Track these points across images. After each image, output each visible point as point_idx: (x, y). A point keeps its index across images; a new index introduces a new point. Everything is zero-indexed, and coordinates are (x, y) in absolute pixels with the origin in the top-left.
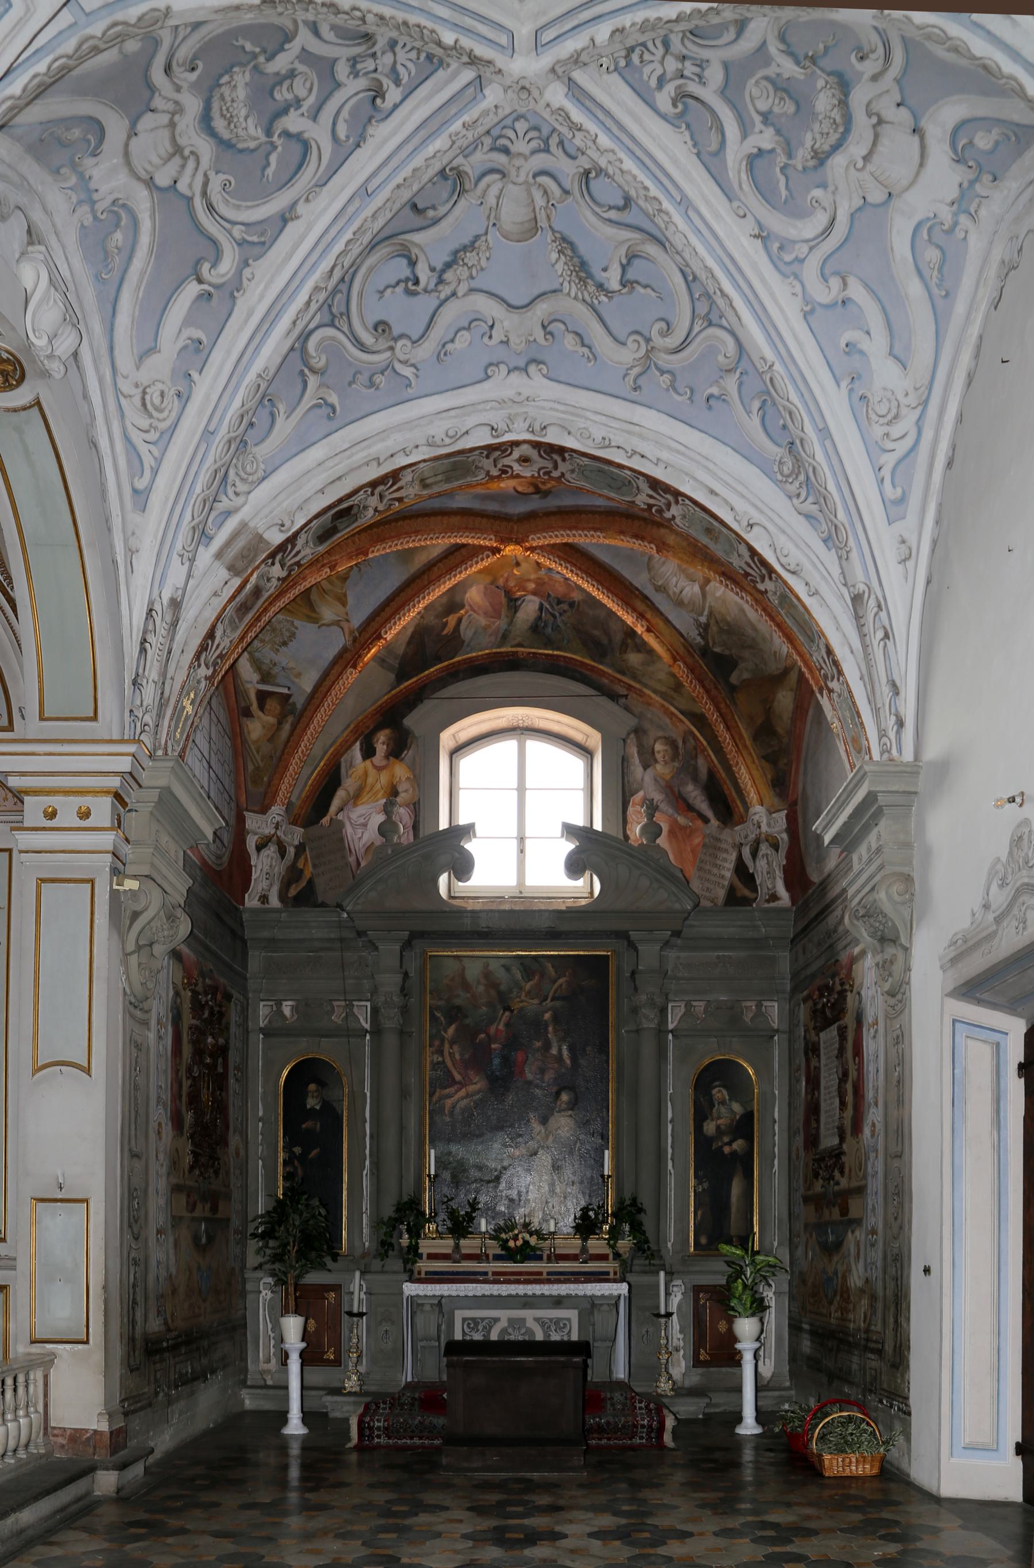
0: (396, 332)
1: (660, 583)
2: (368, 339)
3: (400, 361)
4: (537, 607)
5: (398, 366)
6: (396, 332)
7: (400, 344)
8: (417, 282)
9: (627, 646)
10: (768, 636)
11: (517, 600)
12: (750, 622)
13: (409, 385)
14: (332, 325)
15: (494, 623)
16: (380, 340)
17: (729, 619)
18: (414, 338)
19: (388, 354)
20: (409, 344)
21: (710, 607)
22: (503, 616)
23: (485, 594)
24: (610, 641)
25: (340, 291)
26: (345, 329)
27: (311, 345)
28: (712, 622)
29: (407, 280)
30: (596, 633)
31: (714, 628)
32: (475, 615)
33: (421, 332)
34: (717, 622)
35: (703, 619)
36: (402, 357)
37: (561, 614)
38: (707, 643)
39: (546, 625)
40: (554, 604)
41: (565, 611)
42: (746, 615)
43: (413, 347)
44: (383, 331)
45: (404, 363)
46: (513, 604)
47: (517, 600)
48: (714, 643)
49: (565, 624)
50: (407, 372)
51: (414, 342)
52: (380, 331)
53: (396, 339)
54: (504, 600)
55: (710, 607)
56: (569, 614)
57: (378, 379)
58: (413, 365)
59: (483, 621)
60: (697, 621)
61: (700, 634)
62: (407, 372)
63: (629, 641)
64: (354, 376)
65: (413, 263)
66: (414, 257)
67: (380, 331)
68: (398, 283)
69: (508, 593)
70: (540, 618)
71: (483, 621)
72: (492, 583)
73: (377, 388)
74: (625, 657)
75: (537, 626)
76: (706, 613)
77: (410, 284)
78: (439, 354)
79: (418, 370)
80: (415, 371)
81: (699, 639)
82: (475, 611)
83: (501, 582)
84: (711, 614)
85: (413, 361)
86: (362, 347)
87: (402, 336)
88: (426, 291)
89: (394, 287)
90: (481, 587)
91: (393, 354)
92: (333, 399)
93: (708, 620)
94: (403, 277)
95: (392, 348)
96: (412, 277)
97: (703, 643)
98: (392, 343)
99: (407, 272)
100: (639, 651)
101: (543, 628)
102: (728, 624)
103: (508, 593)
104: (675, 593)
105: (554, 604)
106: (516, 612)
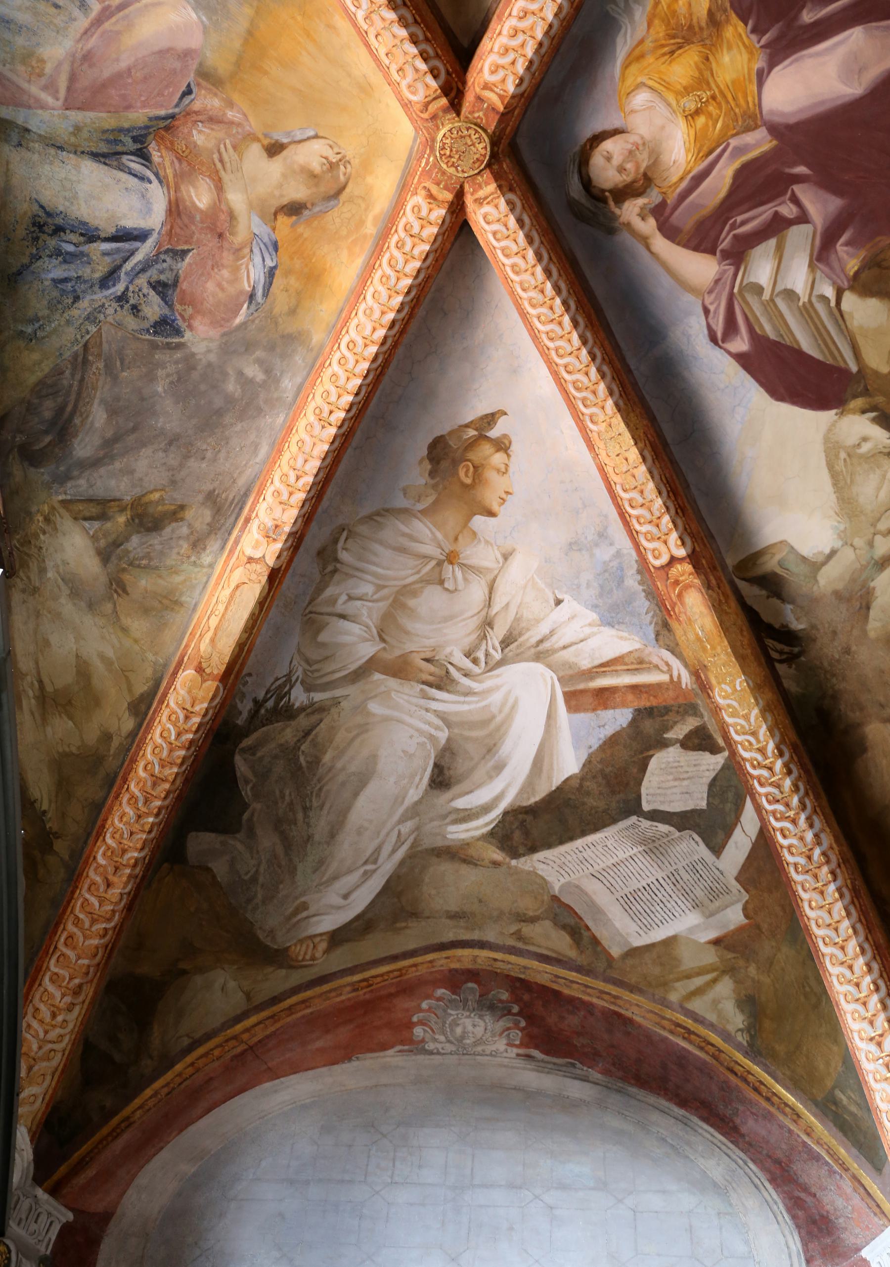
1: (344, 556)
4: (131, 222)
9: (103, 517)
10: (333, 867)
11: (143, 155)
12: (344, 813)
15: (50, 87)
17: (327, 758)
21: (336, 702)
22: (76, 116)
23: (163, 53)
24: (95, 463)
28: (303, 721)
30: (98, 416)
31: (288, 733)
32: (83, 22)
34: (307, 733)
35: (299, 696)
37: (122, 299)
38: (246, 732)
39: (69, 259)
40: (153, 274)
41: (135, 309)
42: (356, 794)
46: (128, 148)
47: (143, 155)
48: (252, 750)
49: (91, 318)
54: (138, 116)
55: (336, 702)
56: (131, 323)
59: (57, 51)
60: (289, 680)
61: (258, 704)
63: (122, 519)
69: (166, 126)
70: (91, 236)
71: (57, 51)
72: (206, 75)
74: (66, 523)
75: (59, 230)
76: (318, 697)
81: (246, 707)
82: (98, 22)
83: (206, 101)
84: (321, 709)
90: (195, 41)
93: (303, 709)
97: (240, 722)
100: (105, 556)
101: (58, 253)
102: (316, 762)
103: (166, 126)
104: (333, 601)
105: (153, 274)
106: (96, 156)
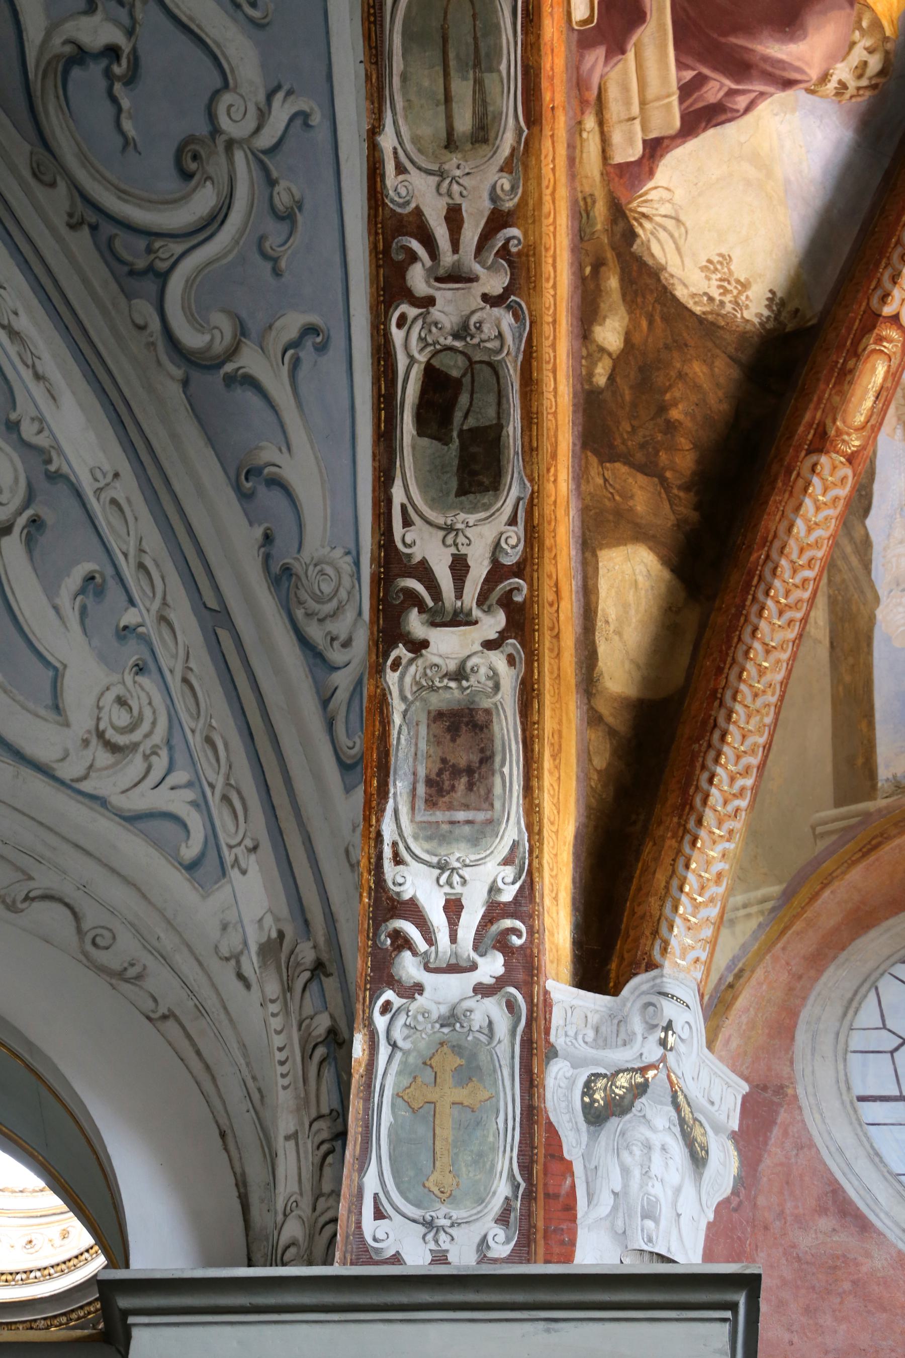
0: (202, 129)
2: (204, 200)
3: (258, 130)
5: (266, 140)
6: (202, 129)
7: (224, 122)
8: (112, 52)
13: (303, 117)
14: (163, 277)
16: (211, 170)
18: (219, 83)
19: (239, 157)
20: (227, 98)
25: (111, 240)
26: (178, 248)
27: (192, 339)
29: (108, 74)
33: (208, 62)
36: (250, 124)
43: (235, 90)
44: (195, 157)
45: (263, 115)
50: (280, 114)
51: (226, 86)
52: (193, 166)
53: (216, 131)
57: (282, 199)
58: (270, 97)
62: (280, 114)
64: (265, 256)
65: (80, 55)
66: (68, 49)
67: (193, 166)
68: (114, 100)
73: (300, 205)
77: (117, 70)
78: (251, 20)
79: (278, 88)
80: (280, 96)
85: (261, 97)
86: (216, 219)
87: (212, 116)
88: (130, 33)
89: (120, 110)
91: (240, 142)
92: (291, 325)
94: (103, 84)
95: (230, 144)
96: (104, 63)
98: (221, 141)
99: (96, 69)
